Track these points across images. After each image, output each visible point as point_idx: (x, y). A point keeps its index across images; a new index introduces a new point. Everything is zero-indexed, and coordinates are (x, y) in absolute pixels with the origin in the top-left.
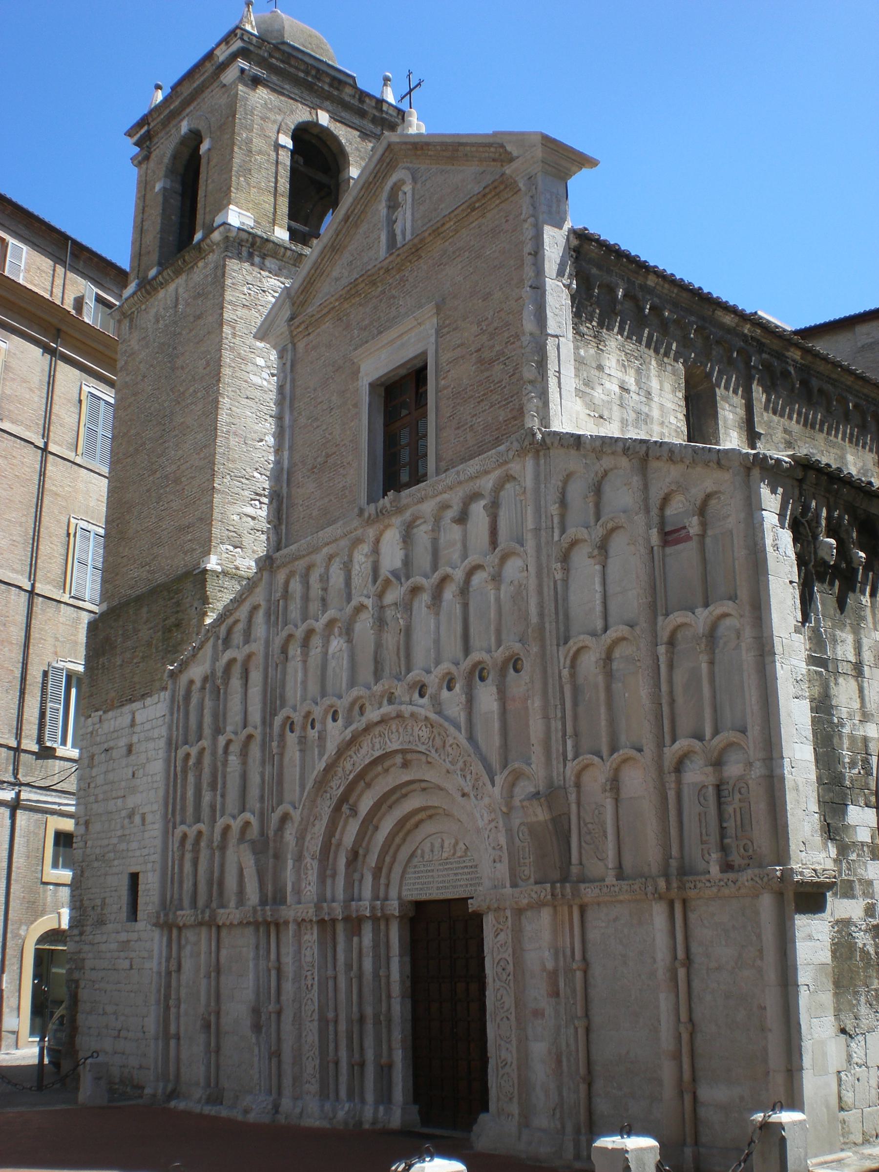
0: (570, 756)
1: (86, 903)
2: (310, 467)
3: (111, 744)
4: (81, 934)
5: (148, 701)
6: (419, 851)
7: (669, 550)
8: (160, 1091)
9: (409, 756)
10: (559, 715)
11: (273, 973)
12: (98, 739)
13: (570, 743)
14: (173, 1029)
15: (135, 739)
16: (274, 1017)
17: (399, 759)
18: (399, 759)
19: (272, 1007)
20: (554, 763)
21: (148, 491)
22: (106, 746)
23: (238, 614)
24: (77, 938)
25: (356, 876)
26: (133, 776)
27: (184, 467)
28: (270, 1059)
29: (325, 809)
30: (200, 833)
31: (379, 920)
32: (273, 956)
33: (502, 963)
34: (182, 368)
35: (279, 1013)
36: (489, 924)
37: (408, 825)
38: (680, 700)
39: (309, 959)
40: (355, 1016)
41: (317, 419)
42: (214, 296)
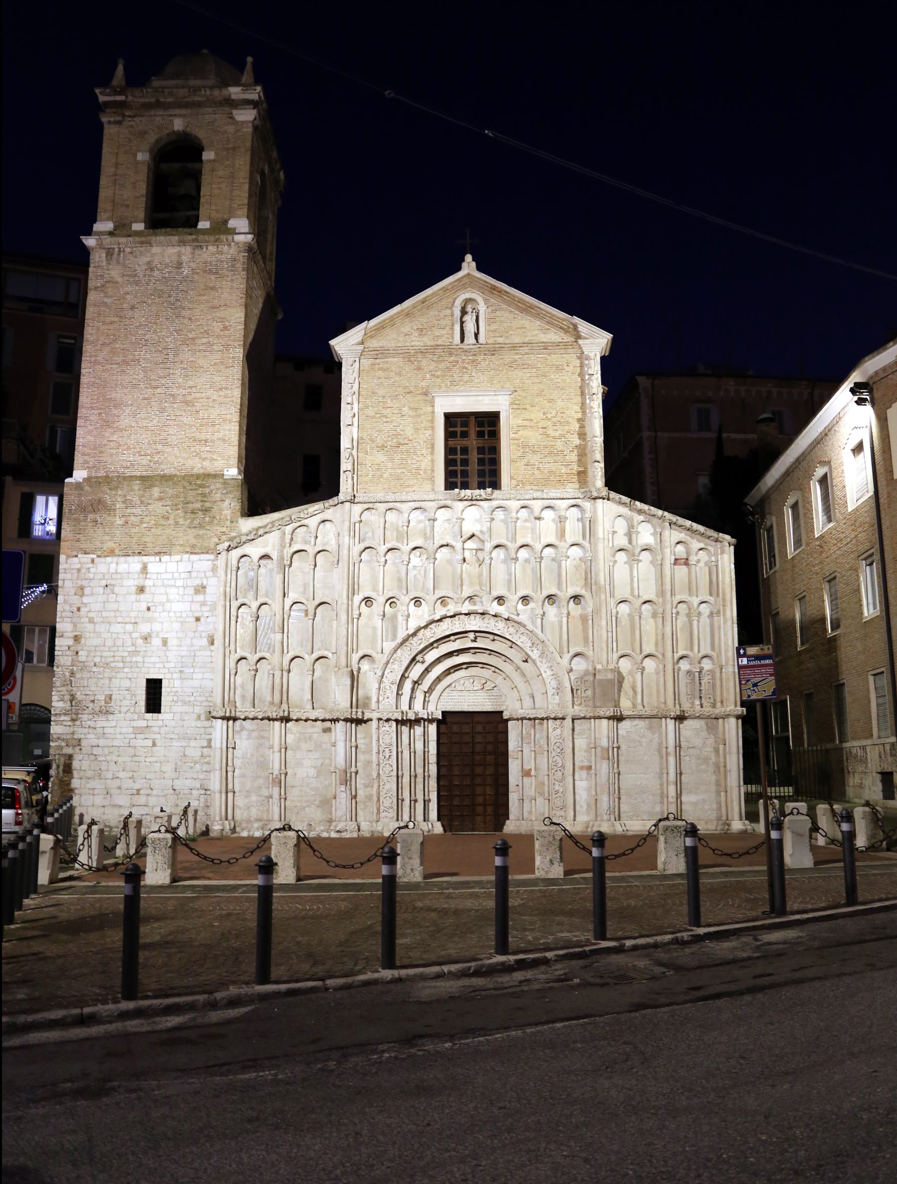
1: (79, 696)
5: (165, 558)
6: (453, 685)
7: (676, 567)
8: (228, 827)
11: (354, 749)
12: (91, 576)
14: (230, 787)
15: (148, 583)
16: (353, 775)
17: (472, 636)
18: (472, 636)
19: (353, 769)
21: (145, 399)
22: (104, 583)
24: (70, 723)
26: (149, 609)
27: (198, 395)
29: (405, 656)
32: (353, 740)
34: (190, 319)
35: (357, 773)
36: (510, 724)
39: (387, 741)
40: (413, 773)
41: (386, 417)
42: (232, 280)
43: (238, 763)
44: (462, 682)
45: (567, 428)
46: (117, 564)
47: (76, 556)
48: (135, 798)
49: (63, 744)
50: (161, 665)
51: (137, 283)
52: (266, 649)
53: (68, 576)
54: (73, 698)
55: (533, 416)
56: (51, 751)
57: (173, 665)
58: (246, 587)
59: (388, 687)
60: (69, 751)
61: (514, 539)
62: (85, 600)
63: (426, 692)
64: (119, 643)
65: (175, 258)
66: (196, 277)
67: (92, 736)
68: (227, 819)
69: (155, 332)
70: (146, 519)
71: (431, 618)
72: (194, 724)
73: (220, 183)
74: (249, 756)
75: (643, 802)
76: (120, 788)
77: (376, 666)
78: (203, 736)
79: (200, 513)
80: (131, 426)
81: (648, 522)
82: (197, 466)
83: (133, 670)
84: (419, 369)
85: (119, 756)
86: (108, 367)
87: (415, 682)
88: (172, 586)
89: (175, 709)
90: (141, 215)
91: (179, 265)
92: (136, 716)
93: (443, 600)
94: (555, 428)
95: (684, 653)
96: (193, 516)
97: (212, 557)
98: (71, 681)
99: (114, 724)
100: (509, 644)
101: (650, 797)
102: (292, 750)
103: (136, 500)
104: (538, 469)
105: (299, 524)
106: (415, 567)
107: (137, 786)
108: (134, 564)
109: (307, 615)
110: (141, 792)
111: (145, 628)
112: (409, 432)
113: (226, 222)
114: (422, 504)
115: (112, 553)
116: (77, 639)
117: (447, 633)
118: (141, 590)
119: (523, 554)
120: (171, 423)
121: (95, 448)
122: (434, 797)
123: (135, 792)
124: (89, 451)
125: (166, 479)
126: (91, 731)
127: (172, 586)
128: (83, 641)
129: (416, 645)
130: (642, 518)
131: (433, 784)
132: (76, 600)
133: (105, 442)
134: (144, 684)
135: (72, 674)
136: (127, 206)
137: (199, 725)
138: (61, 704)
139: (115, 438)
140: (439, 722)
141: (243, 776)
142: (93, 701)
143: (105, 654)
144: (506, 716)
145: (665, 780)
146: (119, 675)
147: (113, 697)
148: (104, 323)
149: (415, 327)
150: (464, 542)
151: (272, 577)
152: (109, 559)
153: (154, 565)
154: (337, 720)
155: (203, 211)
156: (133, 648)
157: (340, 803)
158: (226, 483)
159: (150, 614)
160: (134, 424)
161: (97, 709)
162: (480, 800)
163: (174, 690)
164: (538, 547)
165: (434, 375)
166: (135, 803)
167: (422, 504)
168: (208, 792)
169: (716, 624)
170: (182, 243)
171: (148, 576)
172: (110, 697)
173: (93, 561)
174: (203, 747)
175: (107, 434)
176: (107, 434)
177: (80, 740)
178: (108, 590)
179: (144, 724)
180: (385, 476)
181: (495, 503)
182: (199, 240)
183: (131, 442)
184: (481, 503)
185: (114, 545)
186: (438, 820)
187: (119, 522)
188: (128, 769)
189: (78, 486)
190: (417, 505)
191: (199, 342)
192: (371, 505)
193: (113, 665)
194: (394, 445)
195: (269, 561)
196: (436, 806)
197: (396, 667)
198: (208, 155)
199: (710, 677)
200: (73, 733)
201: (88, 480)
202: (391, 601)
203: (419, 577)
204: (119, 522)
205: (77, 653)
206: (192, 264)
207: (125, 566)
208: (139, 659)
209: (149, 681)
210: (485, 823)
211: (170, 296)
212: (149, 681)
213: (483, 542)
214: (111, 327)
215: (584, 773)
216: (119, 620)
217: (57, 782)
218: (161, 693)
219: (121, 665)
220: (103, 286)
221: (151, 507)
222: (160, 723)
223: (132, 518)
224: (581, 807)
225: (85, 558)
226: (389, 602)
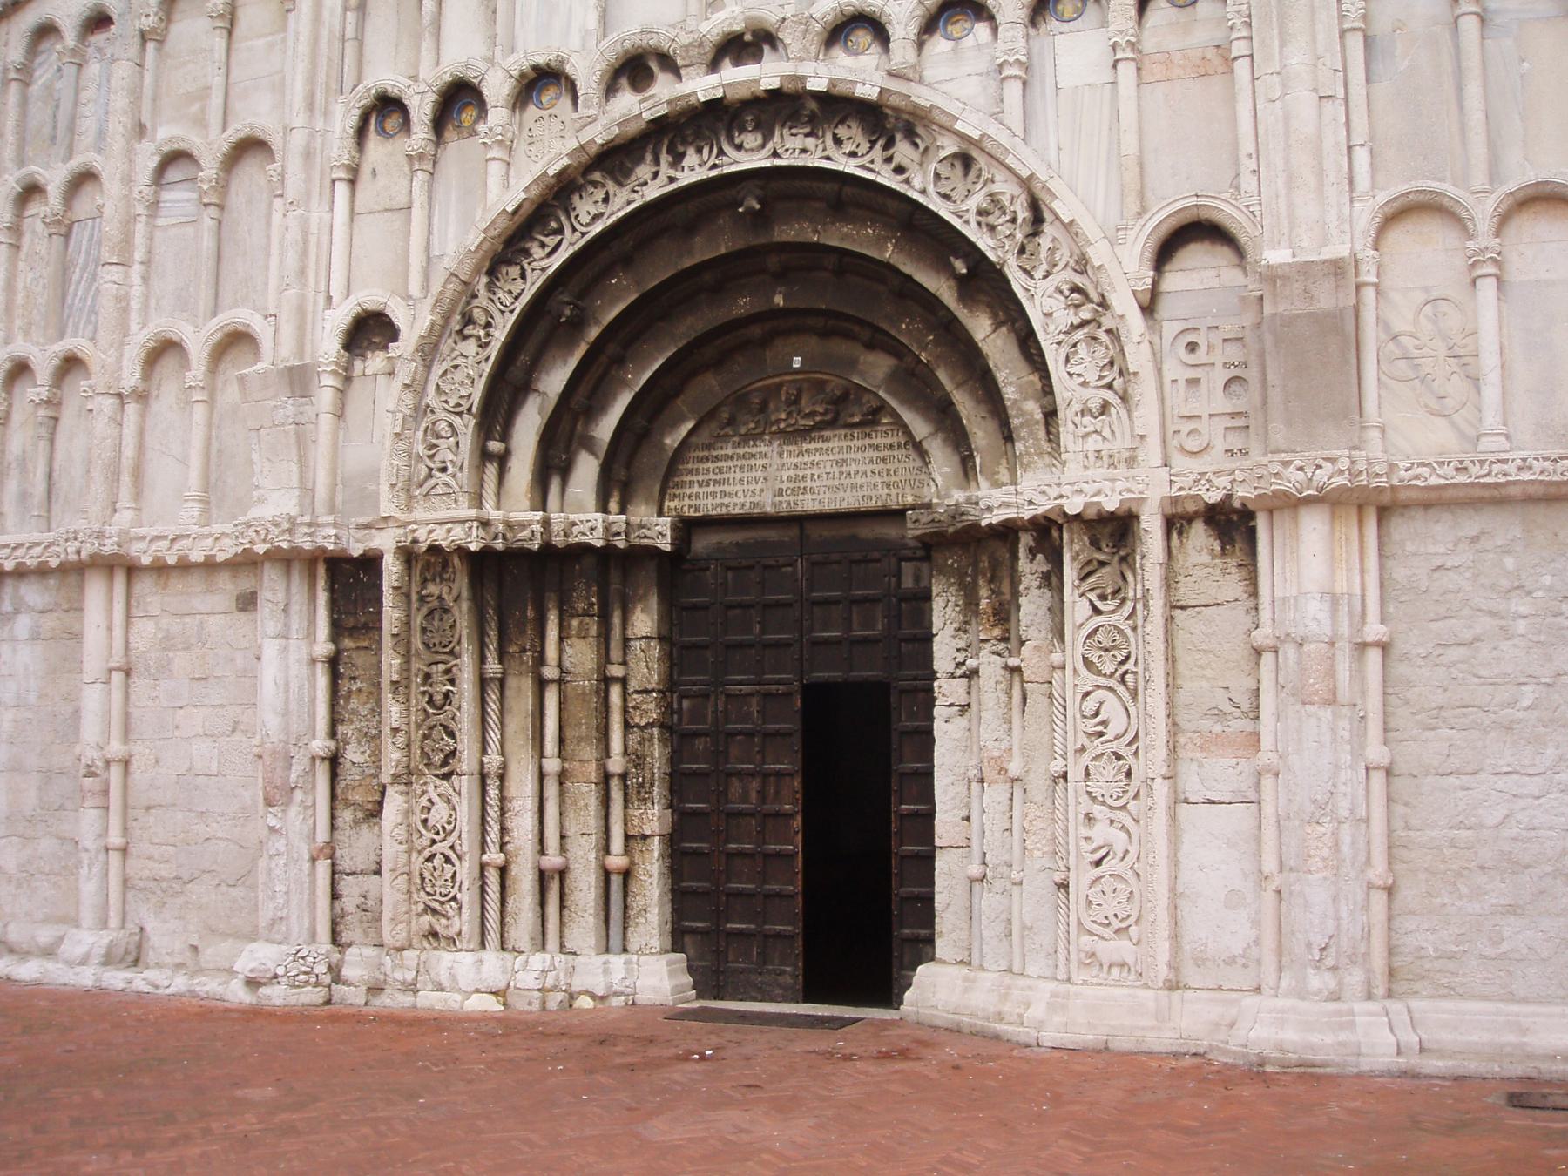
0: (1363, 182)
10: (1341, 94)
13: (1362, 156)
28: (313, 860)
30: (71, 364)
33: (1099, 636)
74: (32, 697)
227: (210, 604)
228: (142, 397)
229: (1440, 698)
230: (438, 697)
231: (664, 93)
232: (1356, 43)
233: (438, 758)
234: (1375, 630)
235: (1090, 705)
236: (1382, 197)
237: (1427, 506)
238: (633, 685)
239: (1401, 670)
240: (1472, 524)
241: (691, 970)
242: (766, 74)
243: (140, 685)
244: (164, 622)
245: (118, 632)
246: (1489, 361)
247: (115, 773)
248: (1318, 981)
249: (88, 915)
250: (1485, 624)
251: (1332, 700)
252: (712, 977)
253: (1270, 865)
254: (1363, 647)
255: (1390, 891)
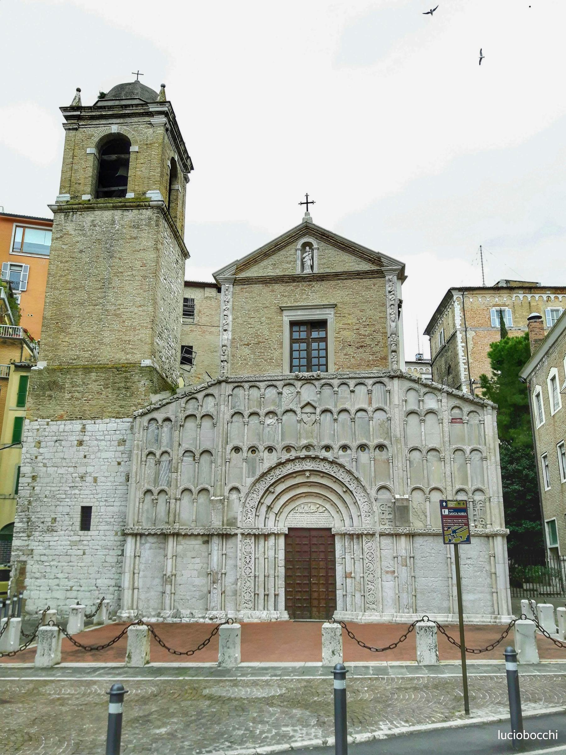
1: (33, 519)
2: (246, 343)
3: (61, 438)
4: (29, 536)
5: (98, 421)
6: (296, 508)
9: (312, 473)
12: (46, 434)
13: (409, 480)
15: (85, 438)
17: (308, 474)
20: (405, 486)
21: (89, 313)
22: (55, 438)
23: (196, 395)
24: (26, 538)
25: (267, 516)
26: (85, 457)
27: (124, 310)
31: (277, 535)
34: (120, 259)
36: (336, 538)
37: (294, 498)
38: (456, 473)
41: (250, 324)
42: (149, 233)
43: (142, 567)
44: (302, 506)
45: (373, 329)
46: (65, 425)
47: (36, 420)
48: (68, 593)
49: (21, 553)
50: (92, 496)
51: (84, 235)
52: (165, 484)
53: (30, 434)
54: (29, 520)
55: (350, 322)
56: (12, 559)
57: (100, 496)
58: (153, 440)
59: (249, 510)
60: (23, 558)
61: (336, 406)
62: (41, 450)
63: (277, 514)
64: (63, 480)
65: (110, 218)
66: (125, 231)
67: (41, 548)
68: (133, 609)
69: (96, 268)
70: (86, 395)
71: (279, 461)
72: (112, 538)
73: (142, 168)
75: (434, 599)
76: (58, 585)
77: (240, 495)
78: (119, 547)
79: (124, 390)
80: (78, 331)
81: (431, 392)
82: (122, 357)
83: (72, 500)
84: (273, 291)
85: (59, 562)
86: (64, 291)
87: (269, 507)
88: (102, 440)
89: (100, 528)
90: (89, 189)
91: (113, 222)
92: (72, 533)
93: (288, 448)
94: (365, 329)
95: (461, 487)
96: (119, 392)
97: (131, 420)
98: (28, 508)
99: (56, 538)
100: (334, 480)
101: (439, 596)
102: (180, 557)
103: (80, 382)
104: (353, 357)
105: (190, 397)
106: (268, 425)
107: (71, 583)
108: (77, 425)
109: (194, 460)
110: (74, 588)
111: (81, 470)
112: (266, 333)
113: (144, 193)
114: (274, 383)
115: (61, 418)
116: (34, 478)
117: (290, 472)
118: (81, 443)
119: (343, 416)
120: (106, 329)
121: (53, 347)
122: (282, 592)
123: (69, 588)
124: (50, 348)
125: (103, 368)
126: (40, 543)
127: (102, 440)
128: (38, 479)
129: (270, 480)
130: (426, 390)
131: (281, 582)
132: (34, 451)
133: (60, 342)
134: (79, 510)
135: (30, 502)
136: (80, 184)
137: (116, 540)
138: (20, 525)
139: (67, 339)
140: (286, 536)
141: (145, 577)
142: (43, 522)
143: (53, 489)
144: (334, 531)
145: (450, 583)
146: (62, 504)
147: (57, 519)
148: (61, 262)
149: (271, 263)
150: (302, 408)
151: (171, 433)
152: (59, 422)
153: (90, 426)
154: (213, 535)
155: (130, 185)
156: (73, 485)
157: (213, 597)
158: (142, 369)
159: (86, 460)
160: (80, 330)
161: (45, 528)
162: (315, 595)
163: (100, 514)
164: (353, 411)
165: (283, 296)
166: (68, 597)
167: (274, 383)
168: (120, 589)
169: (485, 467)
170: (115, 208)
171: (86, 433)
172: (55, 520)
173: (48, 424)
174: (118, 556)
175: (61, 337)
176: (61, 337)
177: (32, 550)
178: (57, 444)
179: (76, 538)
180: (249, 364)
181: (323, 381)
182: (125, 207)
183: (77, 342)
184: (314, 382)
185: (62, 412)
186: (285, 610)
187: (67, 396)
188: (65, 571)
189: (40, 372)
190: (270, 383)
191: (126, 274)
192: (239, 384)
193: (58, 496)
194: (256, 342)
195: (169, 423)
196: (284, 599)
197: (255, 496)
198: (134, 148)
199: (481, 505)
200: (28, 546)
201: (47, 369)
202: (253, 449)
203: (271, 432)
204: (67, 396)
205: (34, 488)
206: (121, 222)
207: (70, 427)
208: (77, 492)
209: (83, 508)
210: (319, 612)
211: (106, 243)
212: (83, 508)
213: (315, 408)
214: (67, 265)
215: (389, 577)
216: (64, 464)
217: (14, 581)
218: (91, 516)
219: (64, 496)
220: (61, 237)
221: (90, 386)
222: (89, 538)
223: (77, 394)
224: (387, 601)
225: (43, 422)
226: (251, 450)
227: (196, 543)
228: (180, 499)
229: (422, 566)
230: (248, 562)
231: (293, 454)
232: (408, 462)
233: (248, 573)
234: (412, 555)
235: (367, 565)
236: (412, 487)
237: (419, 535)
238: (279, 559)
239: (416, 561)
240: (426, 538)
241: (289, 614)
242: (312, 453)
243: (179, 559)
244: (185, 546)
245: (175, 548)
246: (428, 514)
247: (173, 577)
248: (406, 610)
249: (167, 607)
250: (428, 554)
251: (406, 566)
252: (293, 615)
253: (397, 592)
254: (411, 557)
255: (415, 596)
